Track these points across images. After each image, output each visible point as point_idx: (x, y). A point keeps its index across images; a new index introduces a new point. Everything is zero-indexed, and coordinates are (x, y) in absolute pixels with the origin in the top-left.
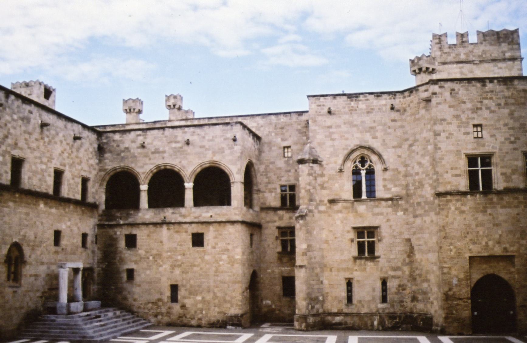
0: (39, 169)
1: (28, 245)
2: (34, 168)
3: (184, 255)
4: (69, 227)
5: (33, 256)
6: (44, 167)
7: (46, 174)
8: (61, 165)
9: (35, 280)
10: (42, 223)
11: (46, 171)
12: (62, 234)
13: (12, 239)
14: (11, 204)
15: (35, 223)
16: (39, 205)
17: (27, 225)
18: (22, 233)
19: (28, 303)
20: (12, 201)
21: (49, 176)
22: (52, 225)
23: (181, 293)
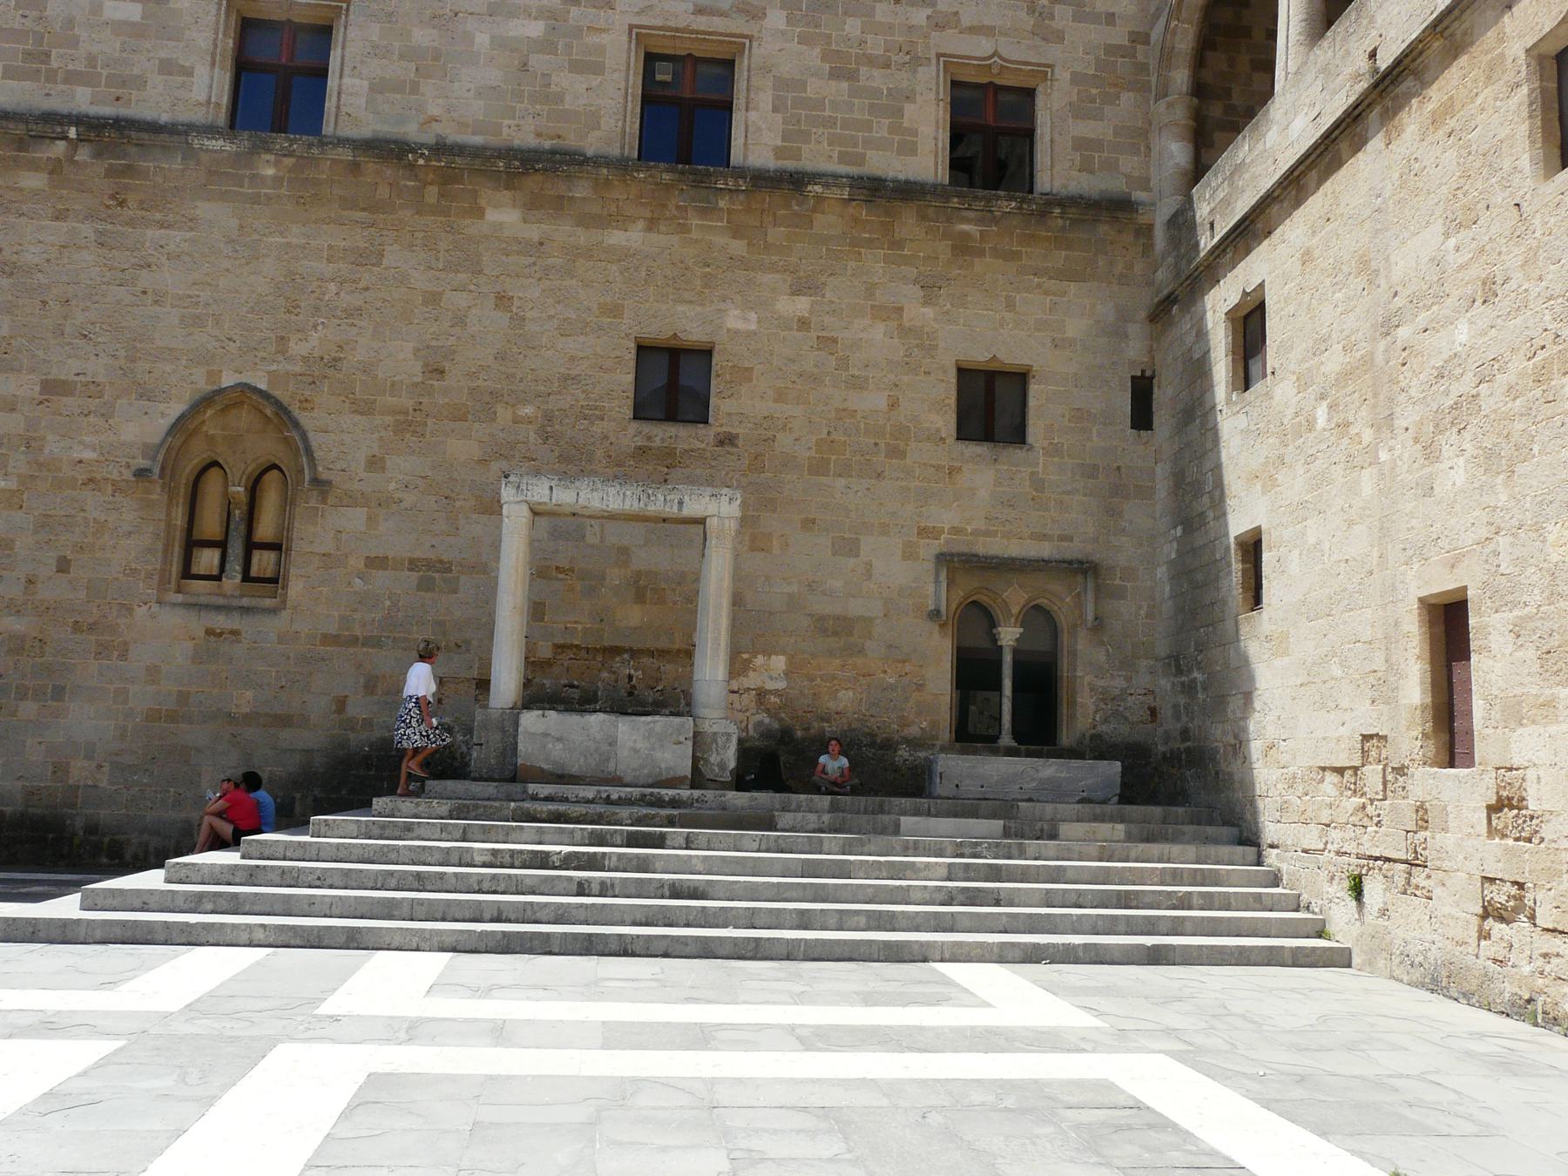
0: (482, 39)
1: (365, 409)
2: (423, 37)
3: (1489, 290)
4: (803, 324)
5: (403, 466)
6: (536, 29)
7: (537, 61)
8: (699, 11)
9: (425, 585)
10: (503, 301)
11: (546, 45)
12: (716, 359)
13: (213, 376)
14: (205, 209)
15: (433, 299)
16: (479, 213)
17: (353, 313)
18: (297, 348)
19: (341, 703)
20: (223, 196)
21: (589, 66)
22: (615, 310)
23: (1493, 667)
